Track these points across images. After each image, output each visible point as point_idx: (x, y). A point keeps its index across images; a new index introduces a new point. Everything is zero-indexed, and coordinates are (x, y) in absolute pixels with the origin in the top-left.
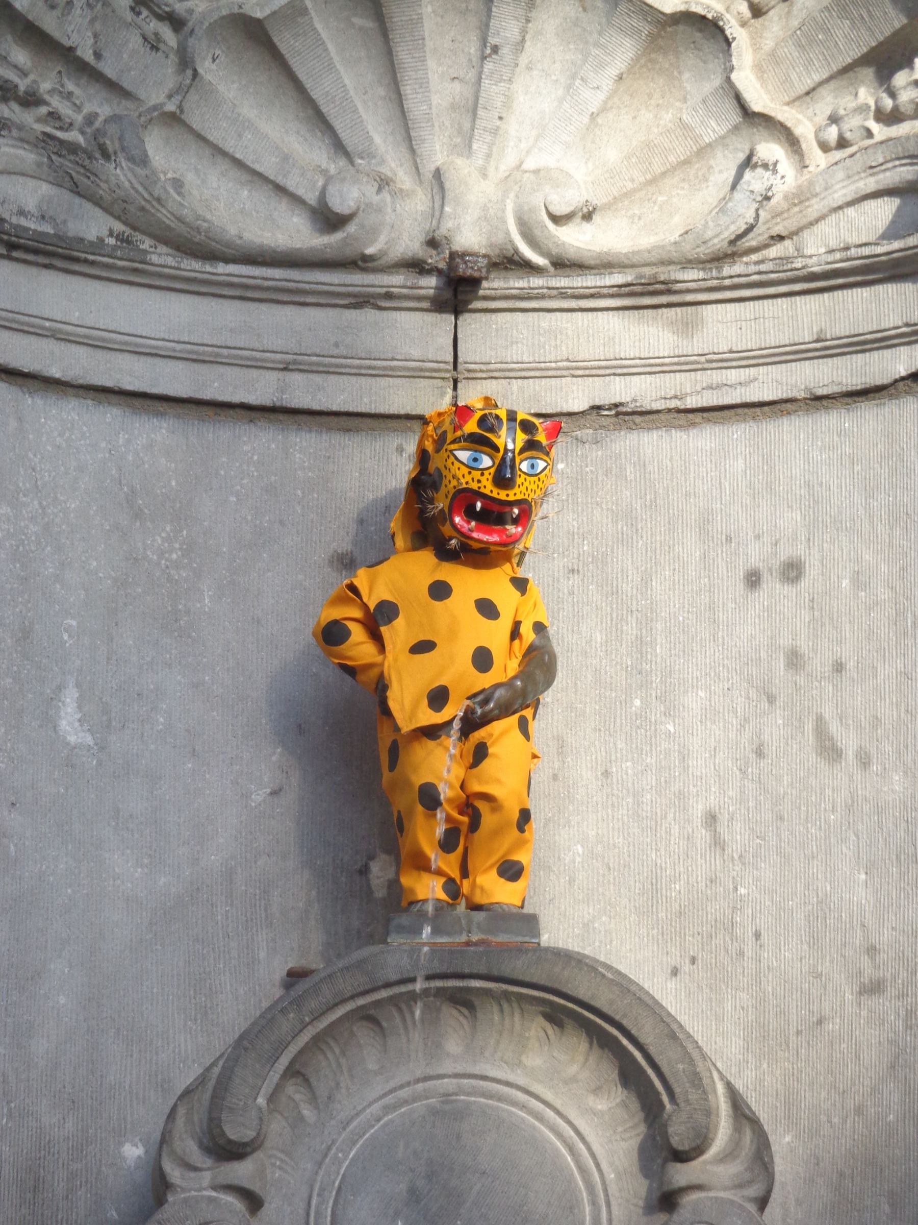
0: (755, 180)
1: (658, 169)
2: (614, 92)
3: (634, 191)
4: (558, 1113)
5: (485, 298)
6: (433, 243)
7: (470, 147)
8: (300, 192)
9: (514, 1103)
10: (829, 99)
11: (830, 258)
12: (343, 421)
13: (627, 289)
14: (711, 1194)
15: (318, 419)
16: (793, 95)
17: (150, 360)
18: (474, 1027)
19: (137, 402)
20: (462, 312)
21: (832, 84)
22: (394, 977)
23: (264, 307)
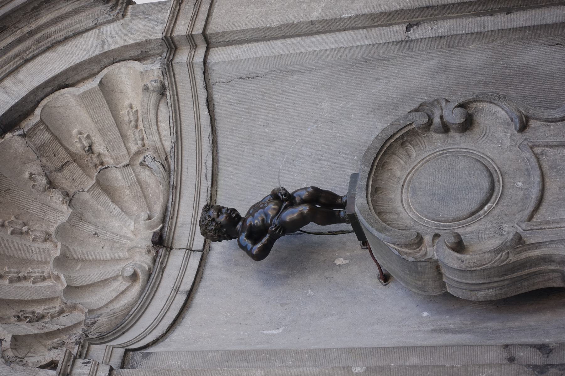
0: (149, 161)
1: (141, 195)
2: (117, 205)
3: (147, 201)
4: (416, 166)
5: (169, 239)
6: (149, 251)
7: (124, 244)
8: (125, 287)
9: (412, 177)
10: (130, 144)
11: (172, 133)
12: (198, 280)
13: (174, 198)
14: (443, 114)
15: (196, 285)
16: (127, 154)
17: (164, 319)
18: (386, 189)
19: (176, 323)
20: (171, 246)
21: (127, 143)
22: (366, 202)
23: (157, 294)
